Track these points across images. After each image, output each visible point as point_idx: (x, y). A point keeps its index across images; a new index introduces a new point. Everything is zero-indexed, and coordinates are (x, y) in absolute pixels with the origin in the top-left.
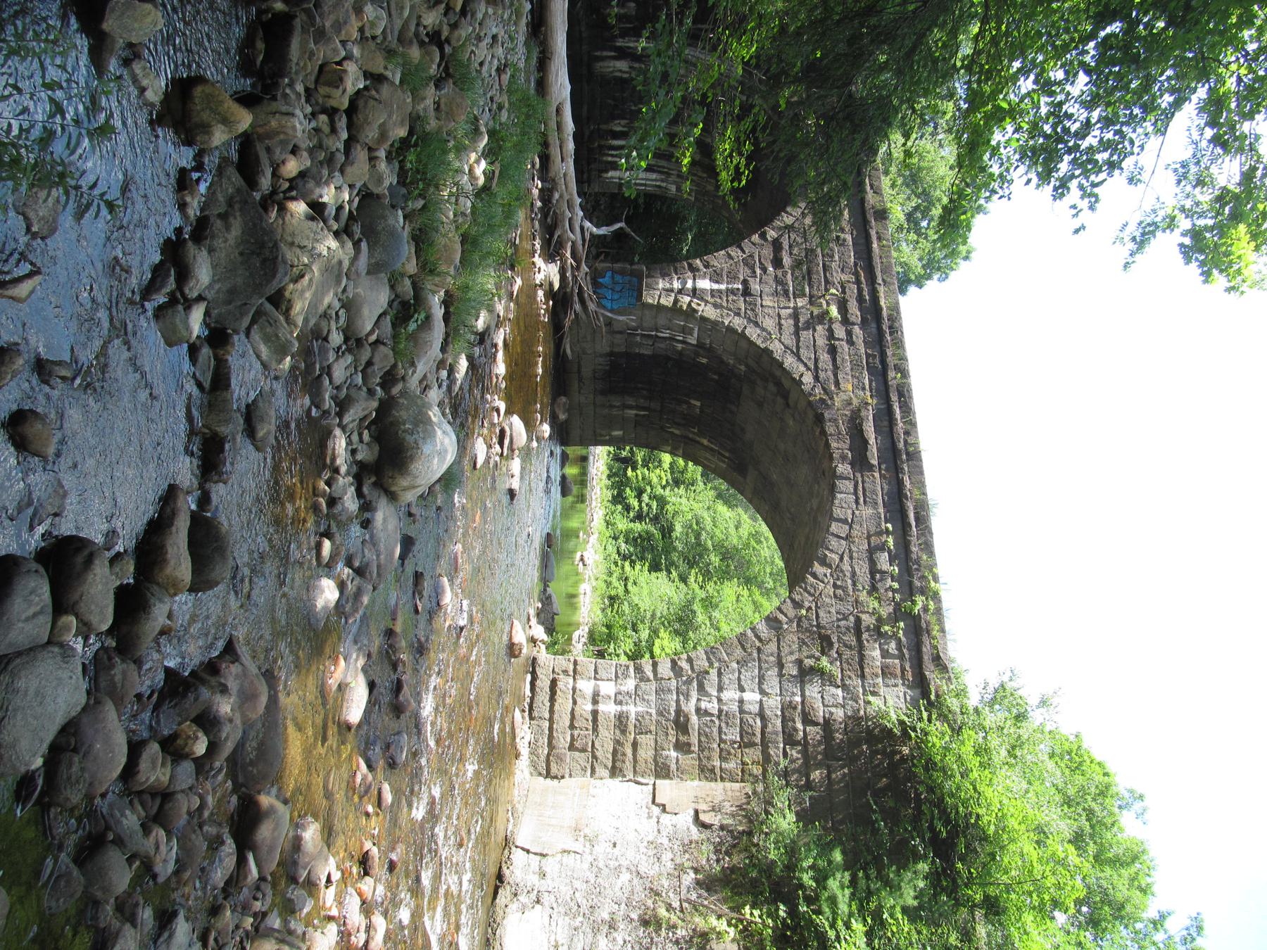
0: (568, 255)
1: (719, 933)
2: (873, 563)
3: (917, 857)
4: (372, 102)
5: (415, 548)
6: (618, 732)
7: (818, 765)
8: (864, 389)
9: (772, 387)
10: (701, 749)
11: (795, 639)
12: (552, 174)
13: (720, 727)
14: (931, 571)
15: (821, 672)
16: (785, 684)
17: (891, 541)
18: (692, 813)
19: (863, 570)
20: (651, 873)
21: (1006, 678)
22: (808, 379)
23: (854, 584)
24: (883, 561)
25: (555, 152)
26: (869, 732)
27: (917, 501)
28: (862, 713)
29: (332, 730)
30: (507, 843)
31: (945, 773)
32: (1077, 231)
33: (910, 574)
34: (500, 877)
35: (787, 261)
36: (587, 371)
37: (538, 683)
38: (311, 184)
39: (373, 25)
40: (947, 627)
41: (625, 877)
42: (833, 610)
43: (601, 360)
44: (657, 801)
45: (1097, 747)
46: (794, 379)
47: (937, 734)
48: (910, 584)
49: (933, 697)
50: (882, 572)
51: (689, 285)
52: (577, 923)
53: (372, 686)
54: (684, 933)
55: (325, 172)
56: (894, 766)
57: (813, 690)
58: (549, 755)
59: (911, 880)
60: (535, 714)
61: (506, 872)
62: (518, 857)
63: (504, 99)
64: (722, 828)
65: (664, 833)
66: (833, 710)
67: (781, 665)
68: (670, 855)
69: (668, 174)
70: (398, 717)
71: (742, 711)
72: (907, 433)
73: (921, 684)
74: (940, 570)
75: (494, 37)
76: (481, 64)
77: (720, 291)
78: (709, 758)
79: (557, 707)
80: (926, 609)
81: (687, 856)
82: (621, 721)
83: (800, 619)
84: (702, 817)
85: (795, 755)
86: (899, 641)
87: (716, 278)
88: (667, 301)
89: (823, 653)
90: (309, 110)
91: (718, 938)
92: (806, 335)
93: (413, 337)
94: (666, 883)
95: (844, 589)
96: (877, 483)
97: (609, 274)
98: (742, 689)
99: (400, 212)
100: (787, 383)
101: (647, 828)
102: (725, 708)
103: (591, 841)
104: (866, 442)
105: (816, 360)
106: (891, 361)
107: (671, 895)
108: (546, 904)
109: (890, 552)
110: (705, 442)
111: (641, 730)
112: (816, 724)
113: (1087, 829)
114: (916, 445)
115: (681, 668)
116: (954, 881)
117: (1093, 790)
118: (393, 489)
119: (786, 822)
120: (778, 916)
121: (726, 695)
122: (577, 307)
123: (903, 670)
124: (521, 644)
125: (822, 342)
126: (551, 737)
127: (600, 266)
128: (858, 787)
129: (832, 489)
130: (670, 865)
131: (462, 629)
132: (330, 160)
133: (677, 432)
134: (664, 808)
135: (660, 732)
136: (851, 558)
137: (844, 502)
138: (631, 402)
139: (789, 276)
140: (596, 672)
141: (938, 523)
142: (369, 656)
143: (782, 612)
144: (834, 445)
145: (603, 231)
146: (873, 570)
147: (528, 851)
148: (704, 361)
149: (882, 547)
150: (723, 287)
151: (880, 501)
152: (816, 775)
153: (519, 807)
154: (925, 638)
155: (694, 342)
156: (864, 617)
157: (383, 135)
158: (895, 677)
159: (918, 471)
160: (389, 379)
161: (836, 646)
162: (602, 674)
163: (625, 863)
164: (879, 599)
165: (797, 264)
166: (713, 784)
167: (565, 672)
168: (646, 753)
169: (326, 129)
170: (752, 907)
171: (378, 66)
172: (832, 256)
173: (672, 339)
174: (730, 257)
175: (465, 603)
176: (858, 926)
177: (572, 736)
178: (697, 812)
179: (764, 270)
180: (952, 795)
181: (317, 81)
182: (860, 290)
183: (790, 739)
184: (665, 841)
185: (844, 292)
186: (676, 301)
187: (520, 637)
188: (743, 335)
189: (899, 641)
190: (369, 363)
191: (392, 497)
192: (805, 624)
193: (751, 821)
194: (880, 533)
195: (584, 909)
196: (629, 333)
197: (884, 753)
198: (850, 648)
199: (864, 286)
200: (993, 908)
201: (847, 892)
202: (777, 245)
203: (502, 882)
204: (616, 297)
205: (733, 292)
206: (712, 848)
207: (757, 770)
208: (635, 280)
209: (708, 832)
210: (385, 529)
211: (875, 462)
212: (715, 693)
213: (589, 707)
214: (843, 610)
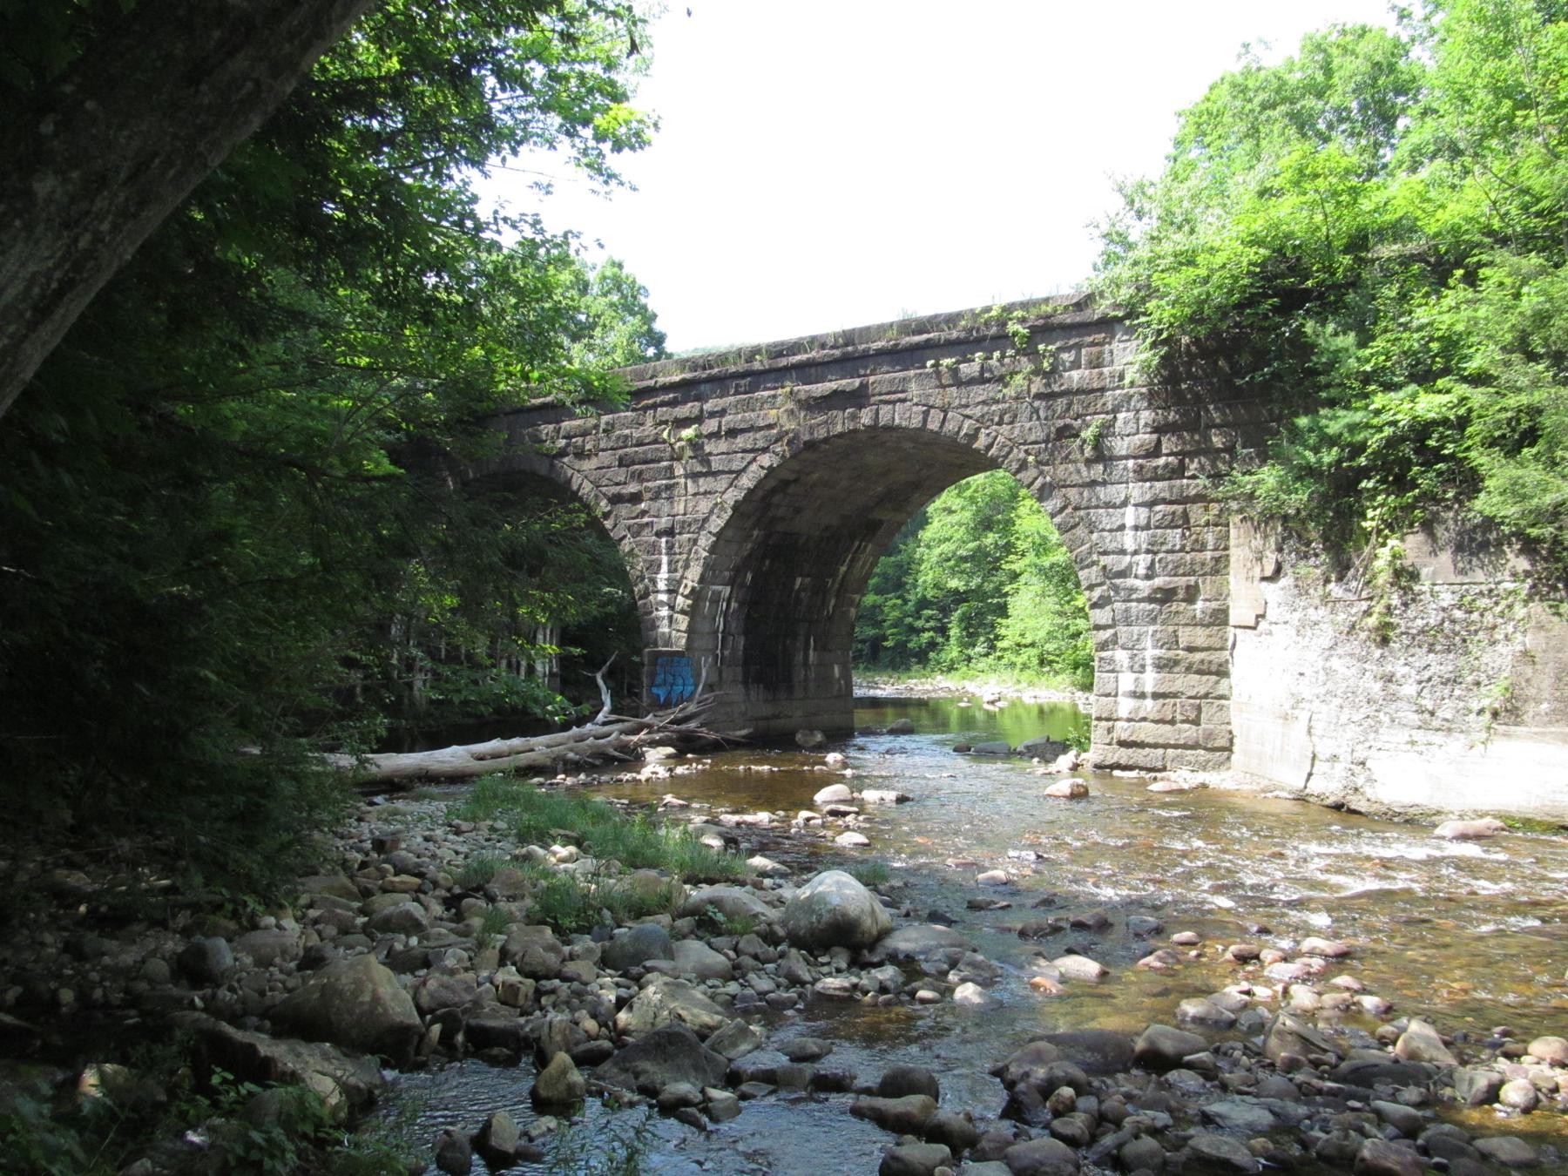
0: (635, 738)
1: (1394, 556)
2: (972, 382)
3: (1299, 332)
4: (527, 959)
5: (940, 911)
6: (1176, 669)
7: (1208, 439)
8: (774, 397)
9: (776, 499)
10: (1193, 573)
11: (1062, 467)
12: (548, 762)
13: (1167, 552)
14: (979, 315)
15: (1099, 439)
16: (1115, 478)
17: (947, 361)
18: (1264, 584)
19: (980, 392)
20: (1331, 633)
21: (1097, 233)
22: (766, 460)
23: (997, 402)
24: (969, 369)
25: (524, 760)
26: (1165, 382)
28: (1144, 390)
29: (1105, 989)
30: (1301, 799)
31: (1205, 301)
32: (601, 246)
33: (984, 338)
34: (1338, 807)
35: (633, 488)
36: (766, 710)
37: (1123, 762)
38: (602, 1010)
39: (460, 960)
40: (1044, 295)
41: (1335, 663)
42: (1028, 425)
44: (1252, 623)
45: (1192, 93)
46: (766, 476)
47: (1161, 312)
48: (995, 338)
49: (1121, 314)
51: (663, 597)
52: (1386, 719)
53: (1070, 951)
54: (1395, 596)
55: (589, 998)
57: (1120, 446)
58: (1206, 749)
59: (1326, 341)
60: (1159, 765)
61: (1331, 800)
62: (1316, 786)
64: (1280, 550)
65: (1288, 617)
66: (1142, 423)
67: (1093, 484)
68: (1311, 611)
70: (1111, 925)
71: (1147, 527)
72: (823, 346)
73: (1107, 325)
74: (978, 305)
75: (427, 839)
76: (457, 853)
77: (670, 563)
78: (1203, 564)
79: (1150, 740)
80: (1023, 320)
81: (1311, 591)
82: (1163, 665)
83: (1039, 463)
84: (1269, 572)
85: (1194, 465)
87: (655, 567)
88: (683, 622)
89: (1077, 436)
90: (538, 1013)
91: (1400, 557)
92: (715, 466)
93: (730, 916)
94: (1342, 617)
96: (881, 379)
97: (655, 690)
98: (1122, 528)
99: (616, 931)
100: (772, 483)
101: (1284, 635)
102: (1144, 546)
103: (1299, 701)
104: (835, 392)
105: (744, 451)
106: (742, 366)
107: (1354, 610)
108: (1365, 754)
109: (958, 362)
110: (843, 569)
111: (1174, 642)
112: (1159, 442)
113: (1283, 108)
114: (836, 336)
115: (1101, 597)
116: (1329, 288)
117: (1238, 103)
118: (875, 932)
119: (1269, 476)
120: (1375, 489)
121: (1130, 545)
122: (692, 725)
123: (1093, 344)
124: (1072, 786)
125: (723, 446)
126: (1185, 747)
127: (646, 701)
128: (1228, 394)
129: (889, 429)
130: (1322, 611)
131: (1039, 857)
132: (578, 994)
133: (833, 602)
134: (1260, 617)
135: (1176, 620)
136: (967, 406)
137: (904, 416)
138: (800, 657)
139: (650, 484)
140: (1108, 695)
141: (925, 307)
142: (1038, 954)
143: (1032, 483)
144: (839, 429)
146: (981, 380)
147: (1310, 775)
148: (749, 576)
149: (954, 371)
150: (665, 559)
151: (901, 374)
152: (1217, 441)
153: (1264, 783)
154: (1055, 320)
156: (1034, 390)
157: (551, 948)
158: (1101, 353)
159: (866, 333)
160: (770, 938)
161: (1068, 421)
162: (1110, 688)
163: (1321, 663)
164: (1013, 374)
165: (639, 476)
166: (1232, 559)
167: (1110, 731)
168: (1200, 636)
169: (553, 998)
170: (1364, 517)
171: (492, 954)
172: (626, 437)
175: (1012, 853)
176: (1379, 400)
177: (1183, 722)
178: (1264, 579)
179: (644, 513)
180: (1230, 292)
181: (514, 1006)
182: (663, 404)
183: (1178, 472)
184: (1297, 615)
185: (666, 422)
186: (683, 612)
187: (1064, 786)
188: (719, 535)
190: (756, 957)
191: (885, 933)
192: (1044, 457)
193: (1272, 517)
194: (938, 374)
195: (1371, 710)
196: (721, 664)
197: (1189, 364)
198: (1070, 405)
199: (658, 400)
200: (1358, 243)
201: (1341, 413)
202: (616, 500)
203: (1342, 805)
205: (670, 548)
206: (1302, 563)
209: (1286, 567)
210: (916, 940)
211: (857, 382)
212: (1128, 558)
213: (1149, 703)
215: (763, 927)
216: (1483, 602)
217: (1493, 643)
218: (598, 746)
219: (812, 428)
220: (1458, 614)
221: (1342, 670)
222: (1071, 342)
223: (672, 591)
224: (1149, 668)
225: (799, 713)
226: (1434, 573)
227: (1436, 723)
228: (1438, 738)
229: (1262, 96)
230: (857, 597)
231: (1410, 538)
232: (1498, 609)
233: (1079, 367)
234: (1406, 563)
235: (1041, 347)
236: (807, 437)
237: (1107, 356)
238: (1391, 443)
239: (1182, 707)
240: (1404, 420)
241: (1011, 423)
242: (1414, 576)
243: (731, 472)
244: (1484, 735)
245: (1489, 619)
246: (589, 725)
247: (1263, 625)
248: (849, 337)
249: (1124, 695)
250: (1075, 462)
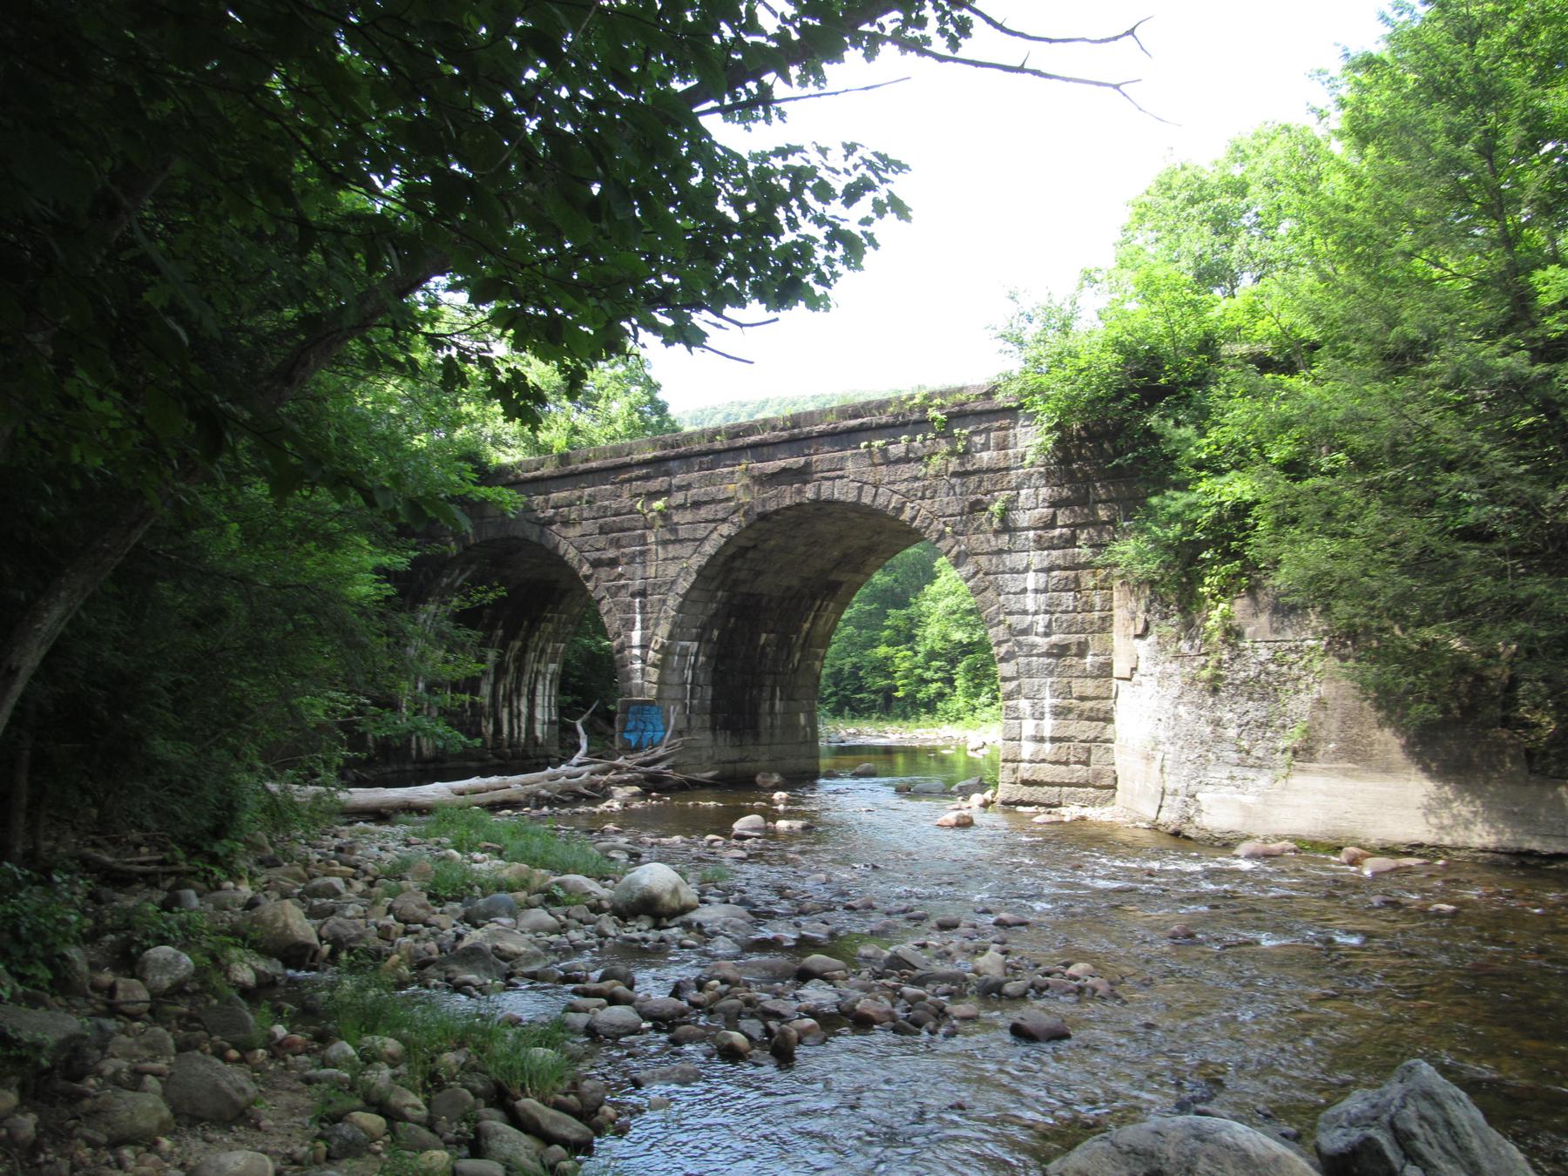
0: (604, 778)
2: (899, 461)
7: (1095, 513)
10: (1083, 631)
12: (522, 798)
15: (1005, 511)
16: (1018, 547)
17: (878, 443)
19: (906, 470)
22: (725, 529)
24: (897, 450)
25: (499, 795)
26: (1060, 462)
27: (838, 417)
30: (1155, 828)
35: (611, 553)
36: (734, 754)
40: (960, 385)
42: (946, 500)
43: (720, 740)
46: (726, 544)
48: (916, 423)
50: (908, 451)
51: (637, 652)
56: (1092, 437)
57: (1022, 519)
60: (1055, 801)
61: (1172, 828)
63: (432, 840)
64: (1148, 611)
65: (1153, 670)
67: (1000, 552)
71: (1045, 591)
72: (774, 428)
75: (381, 849)
77: (643, 621)
79: (1048, 779)
80: (941, 407)
82: (1061, 713)
83: (955, 533)
84: (1139, 632)
85: (1084, 536)
86: (973, 433)
87: (629, 624)
88: (654, 674)
89: (985, 509)
91: (1230, 618)
92: (682, 534)
93: (569, 893)
95: (925, 488)
96: (823, 457)
97: (626, 736)
98: (1024, 591)
100: (731, 550)
104: (784, 470)
105: (707, 521)
112: (1054, 515)
114: (785, 419)
121: (1031, 607)
122: (660, 767)
123: (1000, 429)
125: (688, 516)
126: (1077, 785)
127: (618, 744)
132: (434, 934)
133: (798, 656)
134: (1134, 669)
136: (893, 483)
137: (842, 491)
138: (766, 706)
139: (626, 550)
140: (1013, 740)
144: (787, 502)
145: (584, 743)
146: (906, 460)
148: (716, 633)
149: (884, 451)
150: (638, 617)
152: (1103, 514)
154: (968, 408)
155: (696, 644)
156: (951, 469)
157: (424, 906)
158: (1006, 436)
159: (809, 417)
160: (597, 909)
165: (617, 544)
167: (1015, 771)
168: (1089, 687)
171: (382, 909)
172: (606, 508)
173: (694, 667)
174: (609, 611)
178: (1137, 636)
179: (621, 576)
184: (1159, 668)
185: (639, 495)
186: (654, 665)
188: (685, 596)
189: (973, 433)
190: (581, 921)
192: (960, 527)
194: (871, 454)
195: (1200, 750)
196: (689, 712)
197: (1080, 447)
198: (981, 482)
199: (633, 475)
202: (596, 564)
204: (650, 727)
205: (643, 607)
207: (1102, 573)
208: (632, 709)
209: (1153, 628)
211: (802, 460)
212: (1029, 618)
213: (1047, 746)
214: (945, 490)
215: (593, 901)
216: (1292, 657)
217: (1297, 692)
218: (569, 785)
220: (1272, 667)
221: (1185, 716)
223: (644, 646)
224: (1047, 716)
225: (765, 757)
226: (1255, 632)
227: (1250, 761)
228: (1251, 774)
229: (1185, 194)
230: (821, 651)
231: (1238, 602)
232: (1302, 663)
234: (1235, 623)
235: (956, 431)
236: (759, 509)
237: (1011, 439)
238: (1218, 520)
239: (1072, 751)
240: (1228, 501)
242: (1240, 635)
243: (695, 540)
244: (1286, 771)
245: (1295, 671)
246: (563, 767)
247: (1136, 678)
248: (796, 421)
250: (984, 532)
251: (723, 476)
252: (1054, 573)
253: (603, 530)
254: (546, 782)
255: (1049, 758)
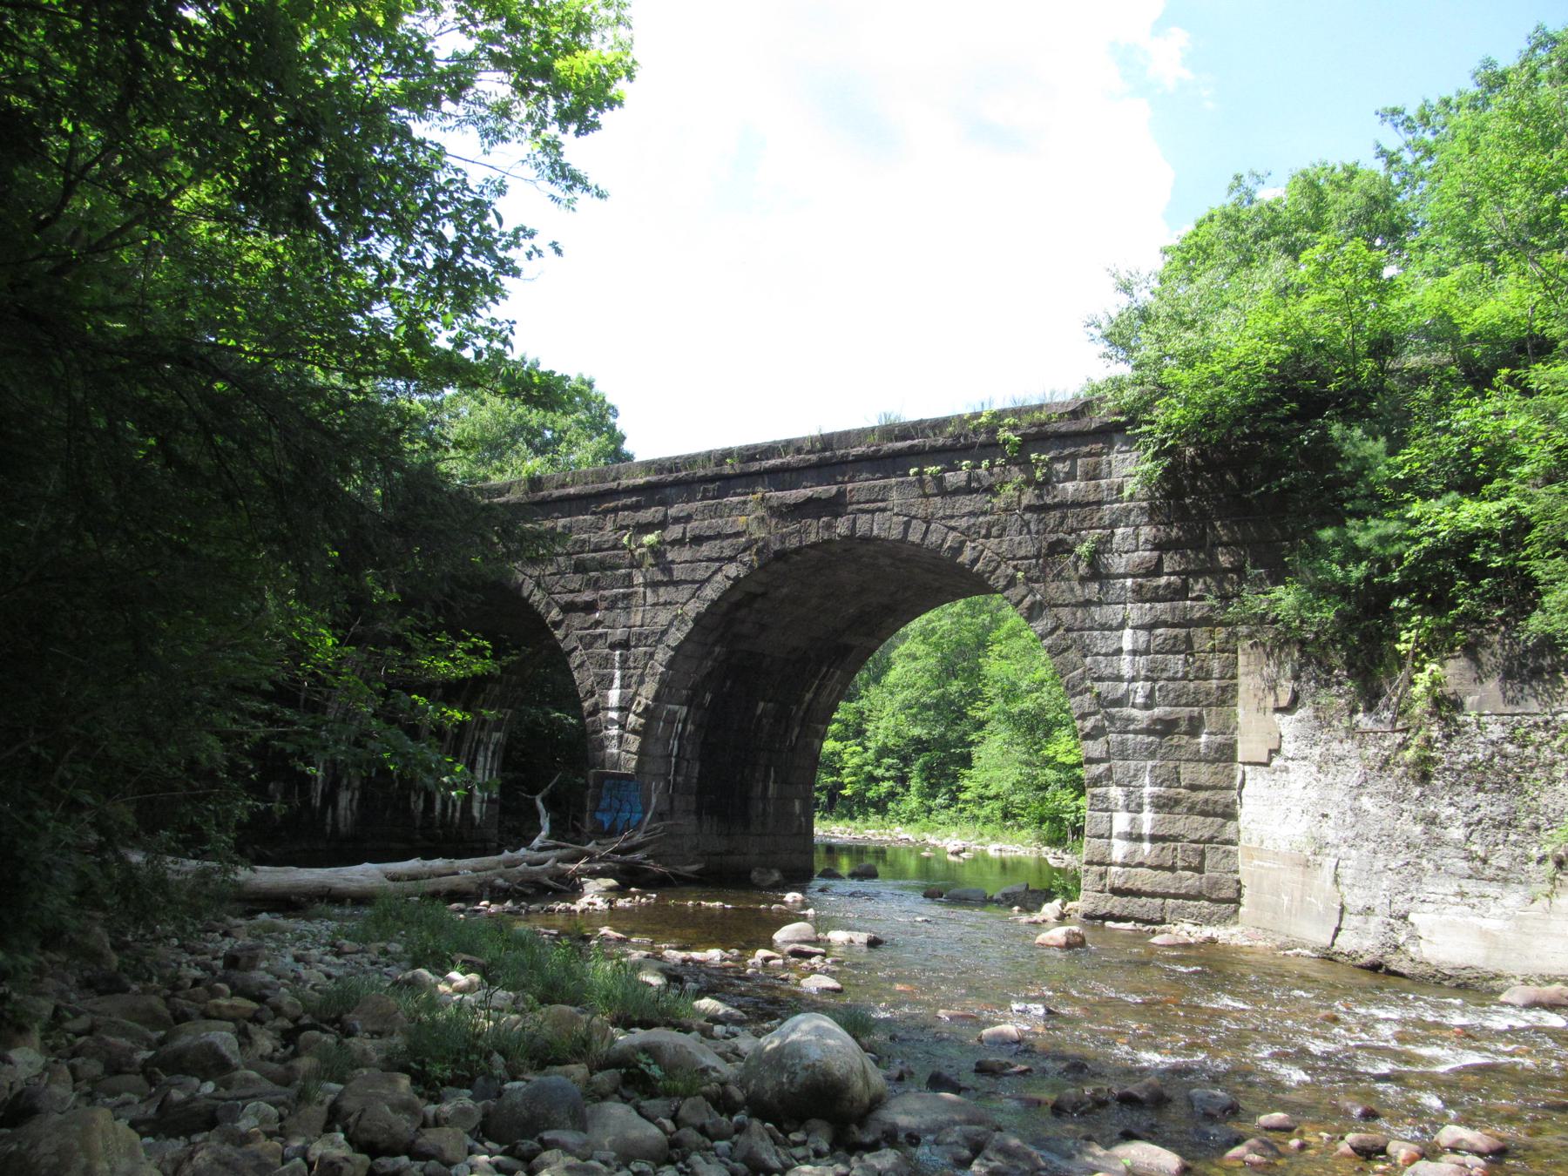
0: (574, 867)
1: (1433, 683)
2: (957, 491)
3: (1325, 437)
4: (364, 1123)
5: (946, 1073)
6: (1178, 809)
7: (1213, 557)
8: (745, 503)
9: (743, 612)
10: (1196, 703)
11: (1054, 585)
12: (473, 888)
13: (1168, 679)
14: (967, 421)
15: (1095, 554)
18: (1278, 715)
19: (966, 503)
20: (1359, 768)
21: (1098, 333)
22: (732, 570)
23: (985, 513)
24: (953, 479)
25: (445, 883)
26: (1167, 496)
28: (1144, 504)
30: (1328, 957)
31: (1216, 404)
32: (558, 252)
33: (972, 446)
34: (1374, 968)
35: (587, 596)
37: (1116, 911)
39: (264, 1120)
40: (1035, 402)
41: (1366, 802)
42: (1017, 539)
44: (1264, 759)
45: (1180, 231)
46: (732, 586)
47: (1169, 413)
48: (983, 446)
49: (1123, 419)
50: (969, 480)
51: (614, 715)
52: (1431, 866)
53: (1128, 1136)
54: (1435, 728)
56: (1210, 465)
57: (1118, 563)
58: (1210, 900)
59: (1355, 445)
60: (1157, 916)
61: (1367, 959)
62: (1346, 942)
63: (375, 947)
64: (1296, 678)
65: (1307, 751)
66: (1142, 539)
67: (1087, 603)
68: (1335, 745)
69: (479, 741)
70: (1170, 1100)
71: (1147, 652)
73: (1108, 433)
74: (966, 411)
75: (297, 959)
76: (329, 976)
77: (623, 678)
78: (1208, 694)
79: (1147, 888)
80: (1014, 428)
81: (1335, 723)
82: (1163, 805)
83: (1029, 580)
84: (1284, 702)
85: (1199, 586)
88: (634, 742)
89: (1071, 551)
91: (1440, 685)
92: (678, 572)
93: (670, 1070)
94: (1372, 750)
95: (990, 526)
96: (860, 486)
97: (598, 816)
98: (1119, 651)
99: (508, 1086)
100: (737, 596)
101: (1300, 774)
102: (1143, 673)
103: (1321, 846)
104: (810, 500)
105: (710, 560)
106: (711, 470)
107: (1386, 744)
108: (1406, 906)
109: (944, 471)
110: (809, 696)
111: (1173, 779)
112: (1160, 561)
113: (1278, 239)
114: (813, 440)
115: (1094, 728)
116: (1351, 393)
117: (1231, 233)
118: (866, 1100)
119: (1286, 597)
120: (1407, 609)
122: (638, 856)
123: (1090, 454)
124: (1068, 934)
125: (686, 553)
126: (1187, 897)
127: (588, 827)
128: (1237, 508)
129: (867, 540)
130: (1347, 745)
131: (1049, 1012)
133: (797, 731)
135: (1177, 755)
136: (952, 517)
137: (884, 526)
138: (759, 789)
139: (606, 593)
140: (1101, 837)
142: (1089, 1139)
143: (1021, 601)
144: (813, 538)
145: (545, 823)
146: (967, 490)
147: (1338, 929)
148: (708, 697)
149: (938, 479)
150: (618, 674)
151: (882, 482)
152: (1224, 560)
153: (1280, 940)
154: (1050, 428)
156: (1025, 501)
157: (407, 1107)
158: (1098, 464)
159: (845, 438)
160: (722, 1103)
161: (1061, 535)
162: (1103, 828)
163: (1348, 802)
164: (1003, 483)
165: (595, 585)
166: (1241, 689)
167: (1102, 876)
168: (1204, 773)
170: (1398, 641)
172: (584, 541)
173: (681, 737)
174: (581, 665)
175: (1015, 1006)
176: (1416, 510)
177: (1184, 869)
178: (1278, 710)
179: (598, 623)
180: (1245, 395)
182: (625, 508)
183: (1181, 593)
184: (1317, 751)
185: (627, 527)
186: (634, 732)
187: (1058, 934)
188: (677, 649)
190: (702, 1130)
191: (877, 1102)
192: (1035, 573)
193: (1287, 642)
194: (921, 482)
195: (1411, 856)
197: (1194, 478)
198: (1063, 518)
199: (620, 503)
200: (1383, 346)
201: (1372, 522)
202: (568, 608)
203: (1380, 966)
205: (624, 661)
206: (1323, 692)
207: (1221, 633)
208: (606, 783)
209: (1303, 695)
211: (834, 489)
212: (1125, 684)
213: (1146, 846)
216: (1538, 736)
217: (1553, 781)
219: (783, 538)
220: (1510, 748)
221: (1374, 810)
222: (1066, 452)
223: (624, 709)
224: (1147, 808)
226: (1481, 703)
227: (1489, 872)
228: (1492, 890)
229: (1252, 229)
231: (1451, 663)
232: (1556, 744)
233: (1074, 478)
234: (1448, 690)
235: (1033, 456)
236: (777, 547)
237: (1104, 467)
238: (1432, 554)
239: (1178, 853)
240: (1444, 530)
241: (1000, 536)
242: (1458, 706)
244: (1549, 887)
245: (1546, 754)
246: (523, 851)
247: (1277, 762)
248: (827, 442)
249: (1119, 836)
250: (1068, 579)
251: (733, 508)
252: (1159, 631)
253: (580, 568)
254: (502, 869)
255: (1148, 862)
